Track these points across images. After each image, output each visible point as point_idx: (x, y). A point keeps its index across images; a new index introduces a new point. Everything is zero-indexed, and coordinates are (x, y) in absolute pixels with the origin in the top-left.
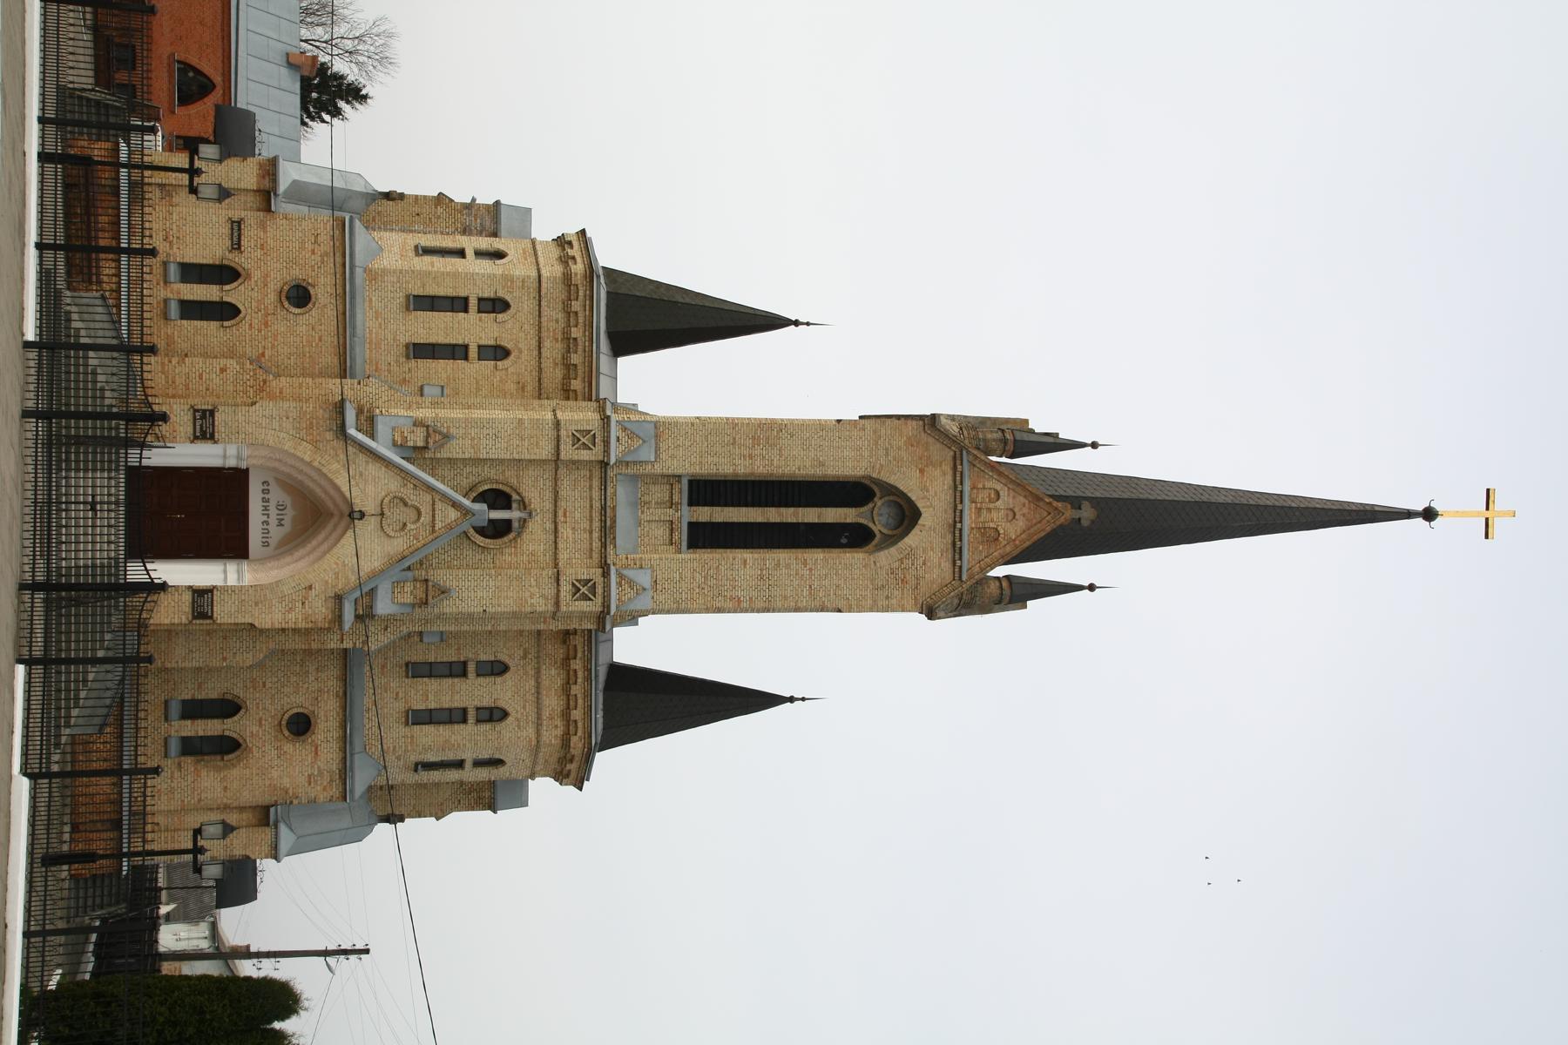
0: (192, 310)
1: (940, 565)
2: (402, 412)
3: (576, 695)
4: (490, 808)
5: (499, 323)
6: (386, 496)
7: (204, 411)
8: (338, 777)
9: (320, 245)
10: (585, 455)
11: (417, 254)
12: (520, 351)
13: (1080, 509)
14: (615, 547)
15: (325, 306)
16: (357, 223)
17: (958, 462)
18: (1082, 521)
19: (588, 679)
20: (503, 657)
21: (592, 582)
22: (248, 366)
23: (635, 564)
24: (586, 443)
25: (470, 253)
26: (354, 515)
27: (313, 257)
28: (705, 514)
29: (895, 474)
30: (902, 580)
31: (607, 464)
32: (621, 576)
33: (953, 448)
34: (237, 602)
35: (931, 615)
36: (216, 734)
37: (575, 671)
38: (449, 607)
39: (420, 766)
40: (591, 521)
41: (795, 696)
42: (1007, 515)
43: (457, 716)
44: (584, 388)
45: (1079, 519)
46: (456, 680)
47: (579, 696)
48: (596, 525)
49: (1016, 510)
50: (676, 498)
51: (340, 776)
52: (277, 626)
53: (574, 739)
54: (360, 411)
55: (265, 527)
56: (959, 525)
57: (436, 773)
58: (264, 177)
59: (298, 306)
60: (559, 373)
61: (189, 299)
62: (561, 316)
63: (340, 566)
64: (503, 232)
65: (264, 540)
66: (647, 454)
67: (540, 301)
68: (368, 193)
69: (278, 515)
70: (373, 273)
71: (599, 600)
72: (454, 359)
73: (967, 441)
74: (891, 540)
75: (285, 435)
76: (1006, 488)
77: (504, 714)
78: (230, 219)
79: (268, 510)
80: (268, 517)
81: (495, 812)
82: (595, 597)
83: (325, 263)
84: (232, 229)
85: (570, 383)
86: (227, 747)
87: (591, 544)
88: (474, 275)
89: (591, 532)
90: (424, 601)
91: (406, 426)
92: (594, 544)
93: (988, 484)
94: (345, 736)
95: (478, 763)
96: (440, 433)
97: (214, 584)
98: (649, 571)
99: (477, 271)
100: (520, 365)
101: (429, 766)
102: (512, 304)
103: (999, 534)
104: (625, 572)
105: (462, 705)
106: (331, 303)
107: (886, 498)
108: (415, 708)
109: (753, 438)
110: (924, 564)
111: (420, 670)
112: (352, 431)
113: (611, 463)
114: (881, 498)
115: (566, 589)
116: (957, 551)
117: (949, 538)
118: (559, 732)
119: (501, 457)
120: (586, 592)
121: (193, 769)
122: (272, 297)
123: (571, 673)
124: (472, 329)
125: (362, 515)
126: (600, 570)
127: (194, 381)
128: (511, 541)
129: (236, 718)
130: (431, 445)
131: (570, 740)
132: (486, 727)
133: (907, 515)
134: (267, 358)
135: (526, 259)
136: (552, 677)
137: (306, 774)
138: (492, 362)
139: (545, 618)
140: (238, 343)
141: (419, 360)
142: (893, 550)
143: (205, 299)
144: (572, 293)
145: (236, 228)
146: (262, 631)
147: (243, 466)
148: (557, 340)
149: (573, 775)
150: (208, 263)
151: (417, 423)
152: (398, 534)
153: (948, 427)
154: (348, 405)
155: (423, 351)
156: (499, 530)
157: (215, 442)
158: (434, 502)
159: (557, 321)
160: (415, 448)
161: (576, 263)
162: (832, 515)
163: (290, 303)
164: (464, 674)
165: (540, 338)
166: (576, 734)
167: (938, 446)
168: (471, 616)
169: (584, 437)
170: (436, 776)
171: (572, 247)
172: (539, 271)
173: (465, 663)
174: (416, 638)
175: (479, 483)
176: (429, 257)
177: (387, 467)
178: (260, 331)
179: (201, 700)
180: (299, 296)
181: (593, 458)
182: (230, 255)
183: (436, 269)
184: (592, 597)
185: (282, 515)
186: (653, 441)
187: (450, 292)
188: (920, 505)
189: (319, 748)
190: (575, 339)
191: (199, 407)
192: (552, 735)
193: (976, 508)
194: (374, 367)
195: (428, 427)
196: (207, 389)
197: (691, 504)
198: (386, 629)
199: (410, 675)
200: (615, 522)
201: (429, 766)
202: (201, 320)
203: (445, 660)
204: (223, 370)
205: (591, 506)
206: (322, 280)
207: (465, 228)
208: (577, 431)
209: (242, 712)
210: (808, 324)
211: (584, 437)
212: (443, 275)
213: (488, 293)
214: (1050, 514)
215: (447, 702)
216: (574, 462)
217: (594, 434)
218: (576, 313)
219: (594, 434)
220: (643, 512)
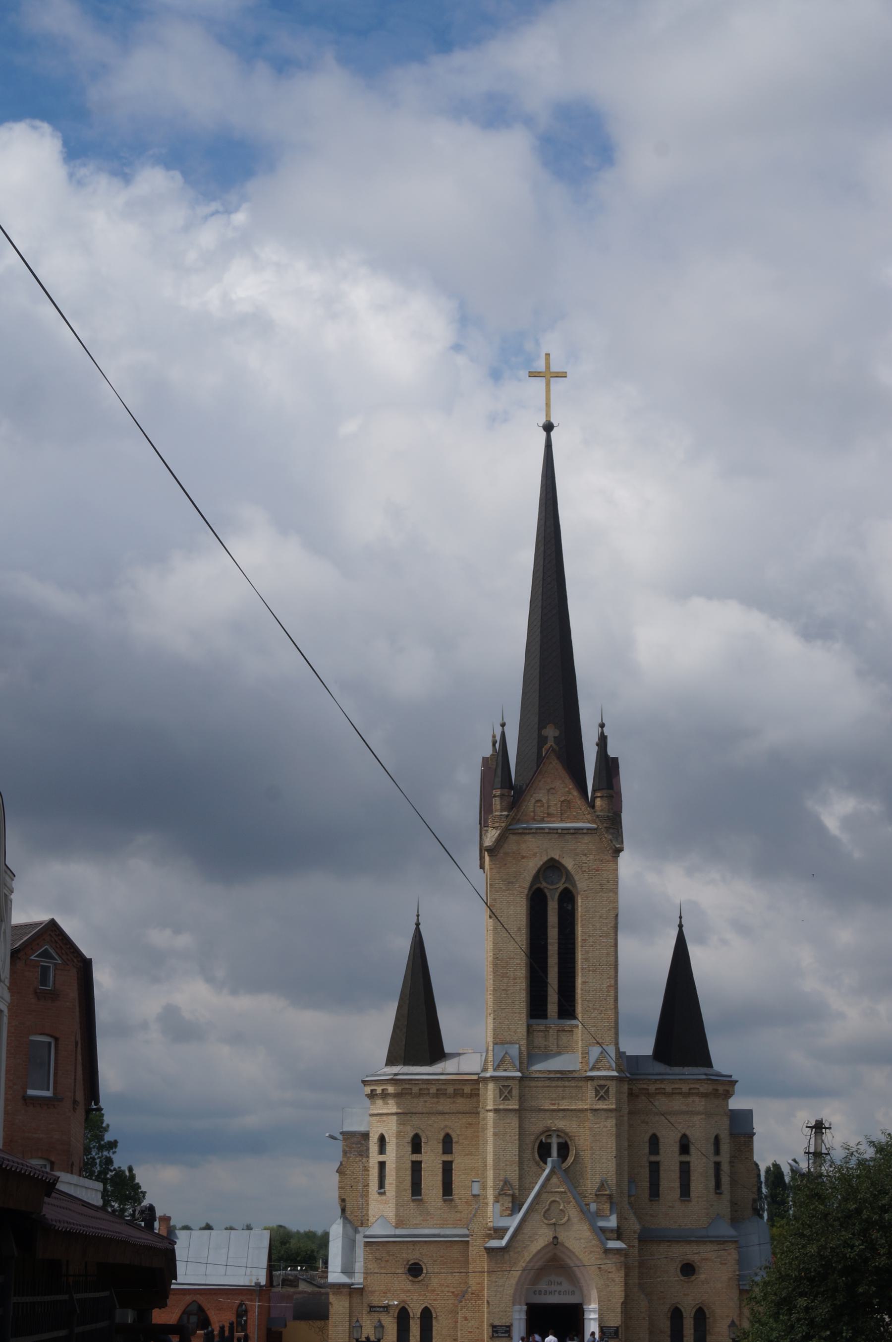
1: (587, 843)
2: (490, 1208)
3: (672, 1089)
4: (752, 1137)
5: (428, 1140)
6: (543, 1222)
7: (493, 1331)
8: (722, 1246)
9: (382, 1257)
10: (515, 1092)
11: (384, 1193)
12: (446, 1126)
13: (547, 737)
14: (574, 1071)
15: (421, 1254)
16: (367, 1233)
17: (516, 831)
18: (556, 736)
19: (662, 1081)
20: (647, 1138)
21: (597, 1087)
22: (463, 1303)
23: (585, 1057)
24: (508, 1091)
25: (382, 1158)
27: (390, 1261)
28: (552, 1008)
29: (525, 876)
30: (597, 871)
31: (521, 1077)
32: (592, 1069)
33: (507, 835)
34: (609, 1312)
35: (621, 850)
36: (693, 1322)
37: (656, 1089)
38: (612, 1181)
39: (718, 1191)
40: (557, 1087)
41: (678, 923)
42: (552, 794)
43: (685, 1170)
44: (469, 1084)
45: (554, 737)
46: (661, 1168)
47: (673, 1087)
48: (560, 1083)
49: (548, 787)
50: (542, 1028)
51: (722, 1244)
52: (623, 1289)
53: (702, 1090)
54: (490, 1237)
55: (562, 1293)
56: (559, 831)
57: (723, 1180)
58: (341, 1292)
59: (421, 1270)
60: (460, 1100)
61: (419, 1338)
62: (422, 1100)
63: (587, 1250)
64: (362, 1129)
65: (570, 1294)
66: (514, 1050)
67: (413, 1113)
68: (343, 1223)
69: (554, 1284)
71: (608, 1083)
72: (452, 1170)
73: (503, 825)
74: (569, 877)
75: (507, 1283)
76: (534, 795)
77: (684, 1137)
78: (368, 1313)
79: (551, 1291)
80: (556, 1291)
81: (754, 1134)
82: (606, 1085)
84: (375, 1311)
85: (466, 1093)
86: (701, 1315)
87: (573, 1087)
89: (565, 1087)
90: (608, 1197)
91: (498, 1205)
92: (573, 1085)
93: (531, 809)
94: (696, 1241)
95: (717, 1152)
96: (503, 1186)
97: (598, 1326)
98: (590, 1048)
99: (394, 1155)
101: (718, 1185)
103: (565, 800)
104: (591, 1066)
105: (678, 1164)
106: (419, 1250)
107: (541, 879)
108: (679, 1195)
109: (502, 977)
110: (585, 855)
111: (655, 1192)
112: (503, 1243)
113: (519, 1074)
114: (541, 883)
115: (602, 1105)
116: (576, 831)
117: (568, 837)
118: (697, 1099)
119: (517, 1145)
120: (603, 1091)
121: (714, 1337)
123: (657, 1092)
125: (555, 1238)
126: (589, 1083)
127: (473, 1336)
128: (571, 1140)
129: (683, 1310)
130: (510, 1192)
131: (702, 1093)
132: (692, 1149)
133: (552, 867)
134: (454, 1290)
135: (384, 1121)
136: (662, 1103)
137: (720, 1266)
138: (453, 1145)
139: (620, 1116)
140: (446, 1308)
141: (453, 1193)
142: (576, 878)
143: (419, 1329)
144: (407, 1092)
145: (374, 1309)
146: (627, 1296)
147: (525, 1307)
148: (438, 1102)
149: (727, 1088)
150: (396, 1326)
152: (567, 1215)
153: (494, 840)
154: (488, 1245)
155: (447, 1189)
156: (564, 1150)
157: (512, 1325)
158: (548, 1192)
159: (426, 1102)
160: (513, 1202)
161: (387, 1089)
162: (553, 918)
163: (420, 1276)
164: (657, 1164)
165: (437, 1113)
166: (698, 1089)
167: (506, 845)
168: (619, 1166)
169: (504, 1093)
170: (725, 1180)
171: (376, 1090)
173: (651, 1163)
174: (633, 1198)
175: (534, 1160)
176: (386, 1186)
177: (525, 1221)
178: (438, 1295)
179: (671, 1331)
180: (415, 1270)
181: (518, 1087)
182: (391, 1312)
183: (394, 1182)
184: (607, 1087)
185: (554, 1282)
186: (506, 1046)
187: (409, 1173)
188: (545, 859)
189: (703, 1257)
190: (438, 1090)
191: (491, 1334)
192: (699, 1104)
193: (547, 817)
194: (459, 1222)
195: (500, 1194)
196: (478, 1328)
197: (544, 1016)
198: (626, 1219)
199: (657, 1198)
200: (558, 1071)
201: (718, 1185)
202: (431, 1330)
203: (648, 1176)
204: (466, 1319)
205: (548, 1086)
206: (405, 1255)
207: (360, 1155)
208: (500, 1098)
209: (679, 1306)
210: (418, 916)
214: (551, 762)
215: (676, 1175)
216: (520, 1098)
217: (502, 1086)
218: (420, 1089)
219: (502, 1086)
220: (552, 1051)
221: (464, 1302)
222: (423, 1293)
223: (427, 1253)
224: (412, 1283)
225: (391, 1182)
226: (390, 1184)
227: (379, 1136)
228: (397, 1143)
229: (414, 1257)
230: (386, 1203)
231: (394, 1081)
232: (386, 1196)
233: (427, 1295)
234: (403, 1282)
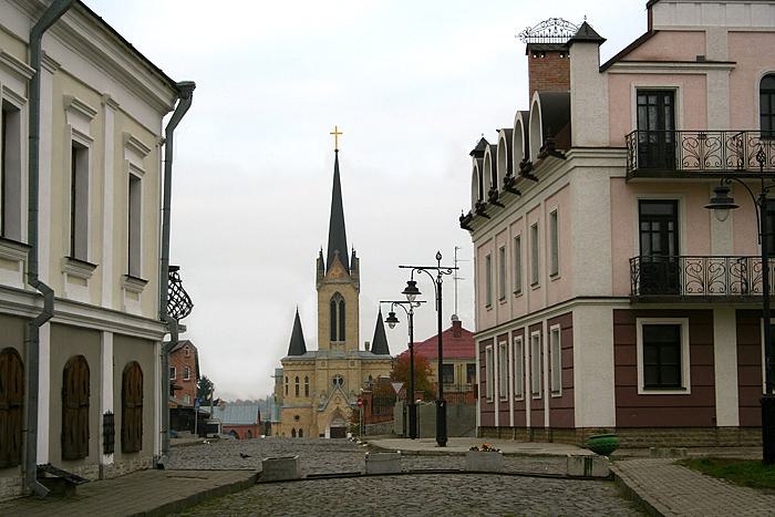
0: (301, 436)
26: (338, 408)
28: (338, 338)
88: (292, 382)
100: (309, 374)
124: (302, 384)
133: (337, 293)
136: (372, 366)
155: (307, 392)
156: (341, 381)
212: (292, 390)
231: (290, 360)
234: (294, 421)
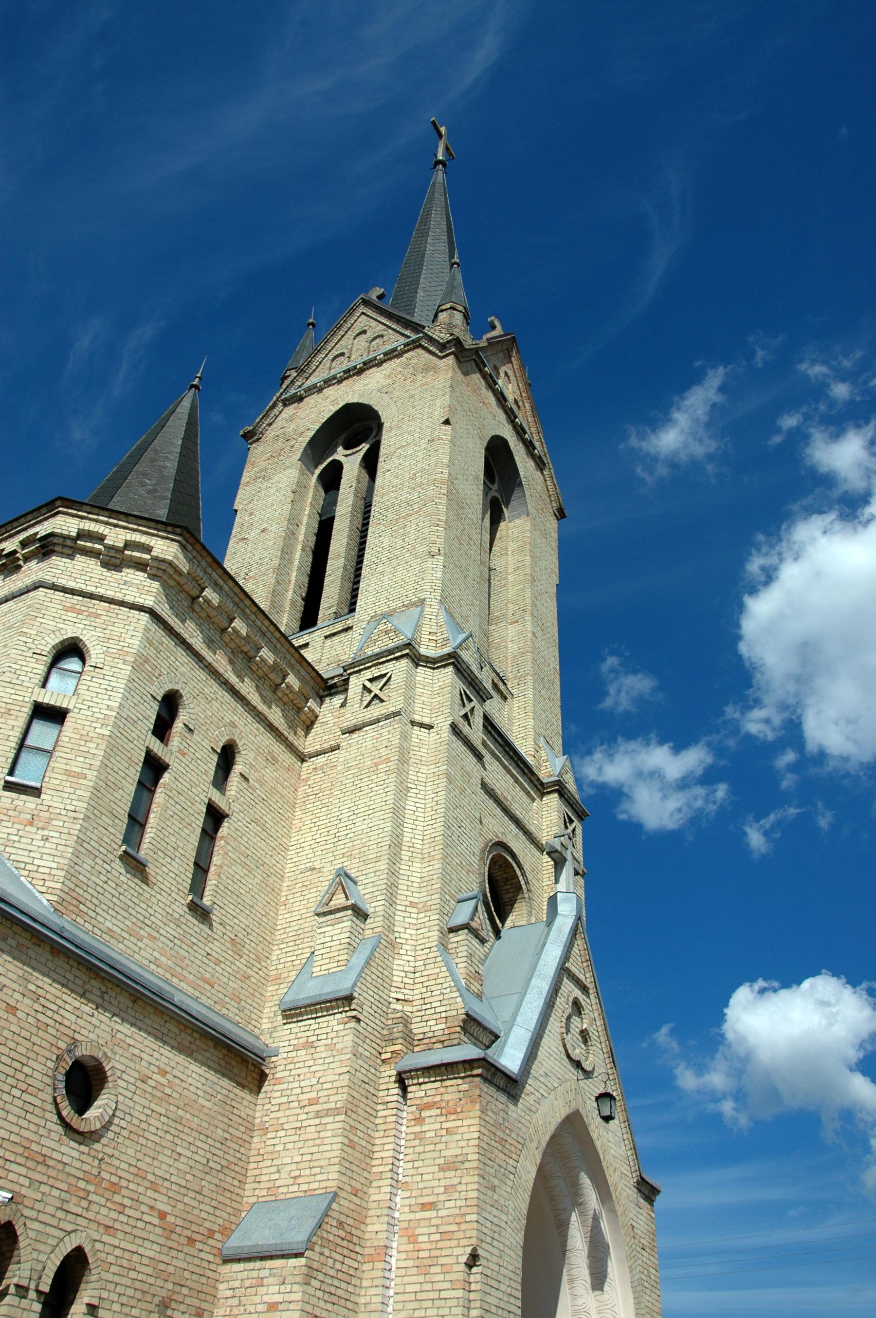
12: (233, 725)
27: (19, 1014)
70: (68, 898)
83: (40, 991)
102: (176, 687)
122: (71, 1150)
134: (168, 1209)
135: (98, 616)
151: (444, 946)
172: (141, 609)
183: (92, 775)
211: (464, 706)
213: (152, 712)
221: (317, 1248)
222: (81, 1184)
223: (131, 1042)
224: (60, 1129)
225: (79, 770)
226: (68, 773)
227: (62, 642)
228: (130, 680)
229: (92, 1036)
230: (31, 824)
232: (38, 801)
233: (92, 1197)
